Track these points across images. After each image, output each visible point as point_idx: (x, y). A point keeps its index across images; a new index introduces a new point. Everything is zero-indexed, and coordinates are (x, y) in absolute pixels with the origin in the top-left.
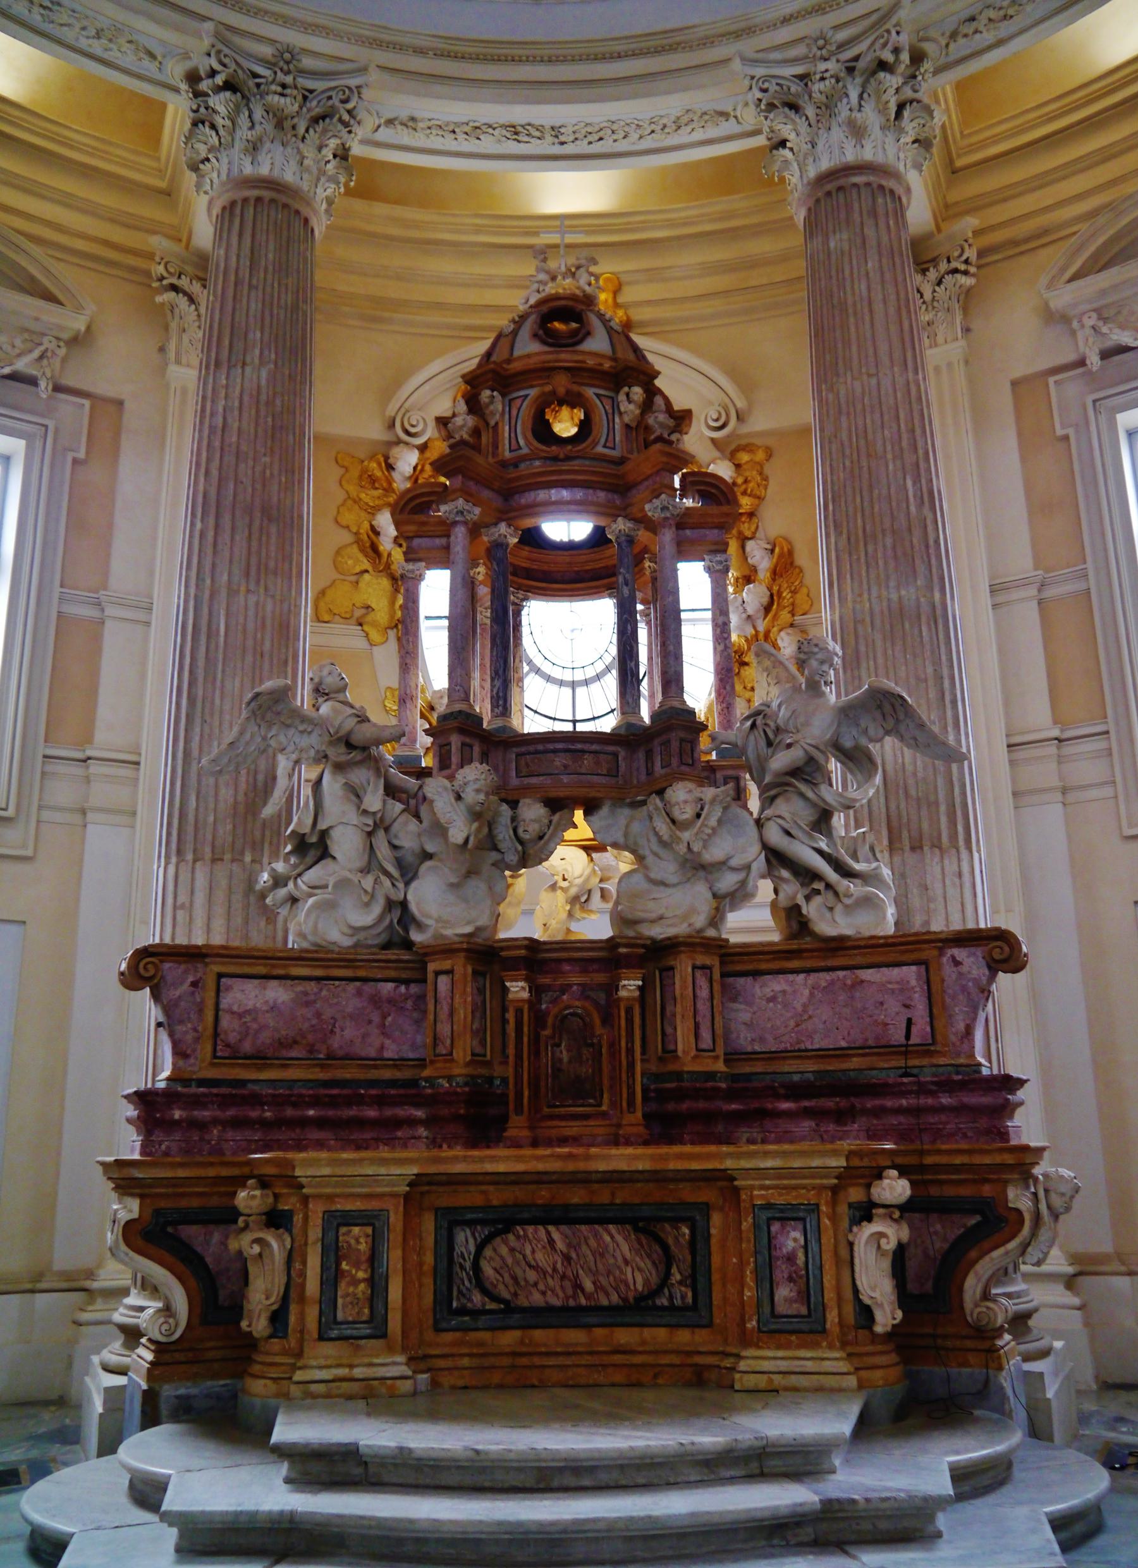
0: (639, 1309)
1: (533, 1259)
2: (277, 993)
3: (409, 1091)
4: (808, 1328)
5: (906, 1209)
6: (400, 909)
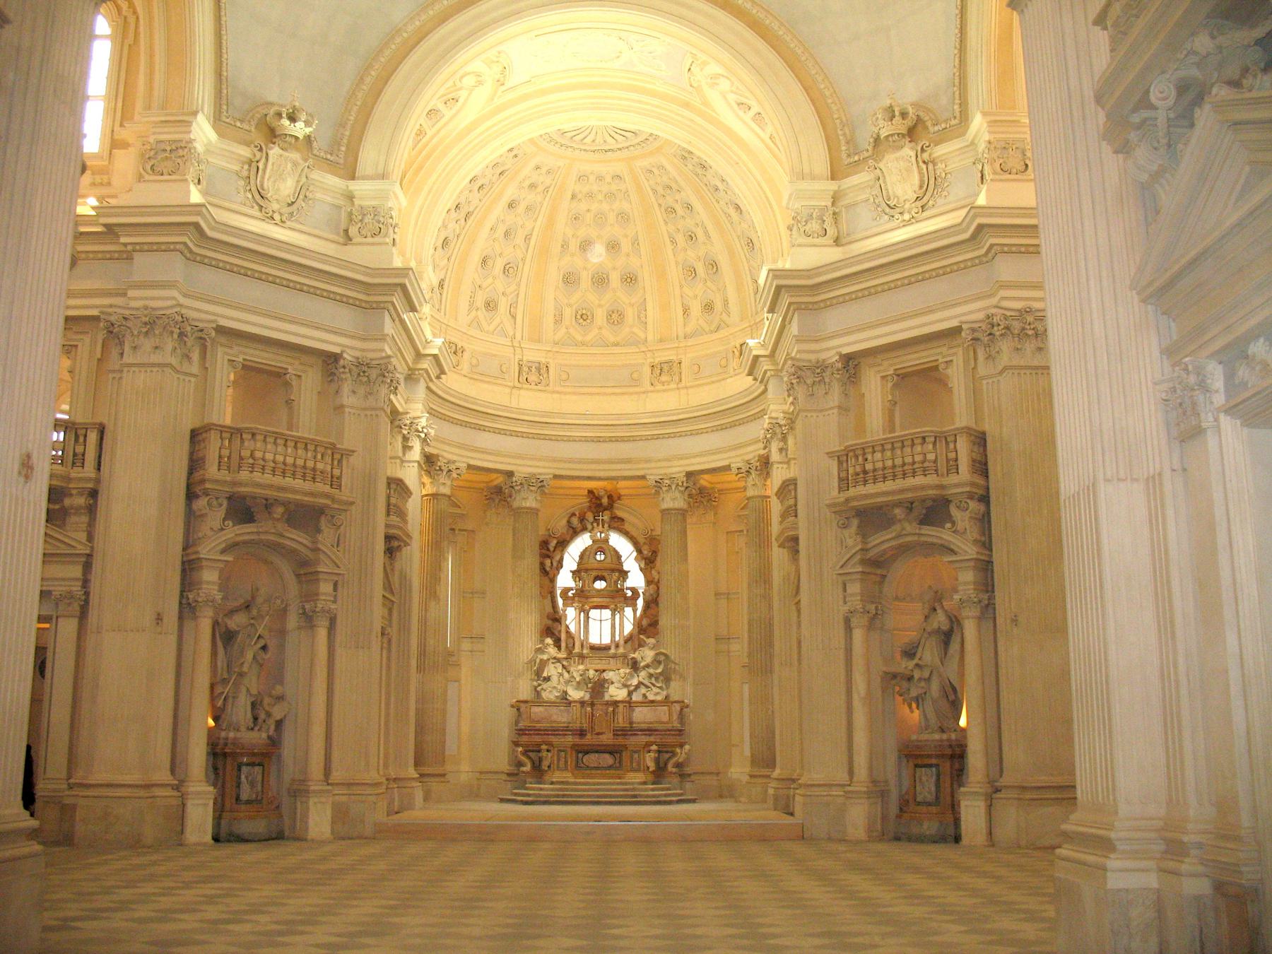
0: (610, 767)
1: (591, 759)
2: (541, 709)
3: (566, 729)
4: (638, 770)
5: (659, 752)
6: (565, 692)
